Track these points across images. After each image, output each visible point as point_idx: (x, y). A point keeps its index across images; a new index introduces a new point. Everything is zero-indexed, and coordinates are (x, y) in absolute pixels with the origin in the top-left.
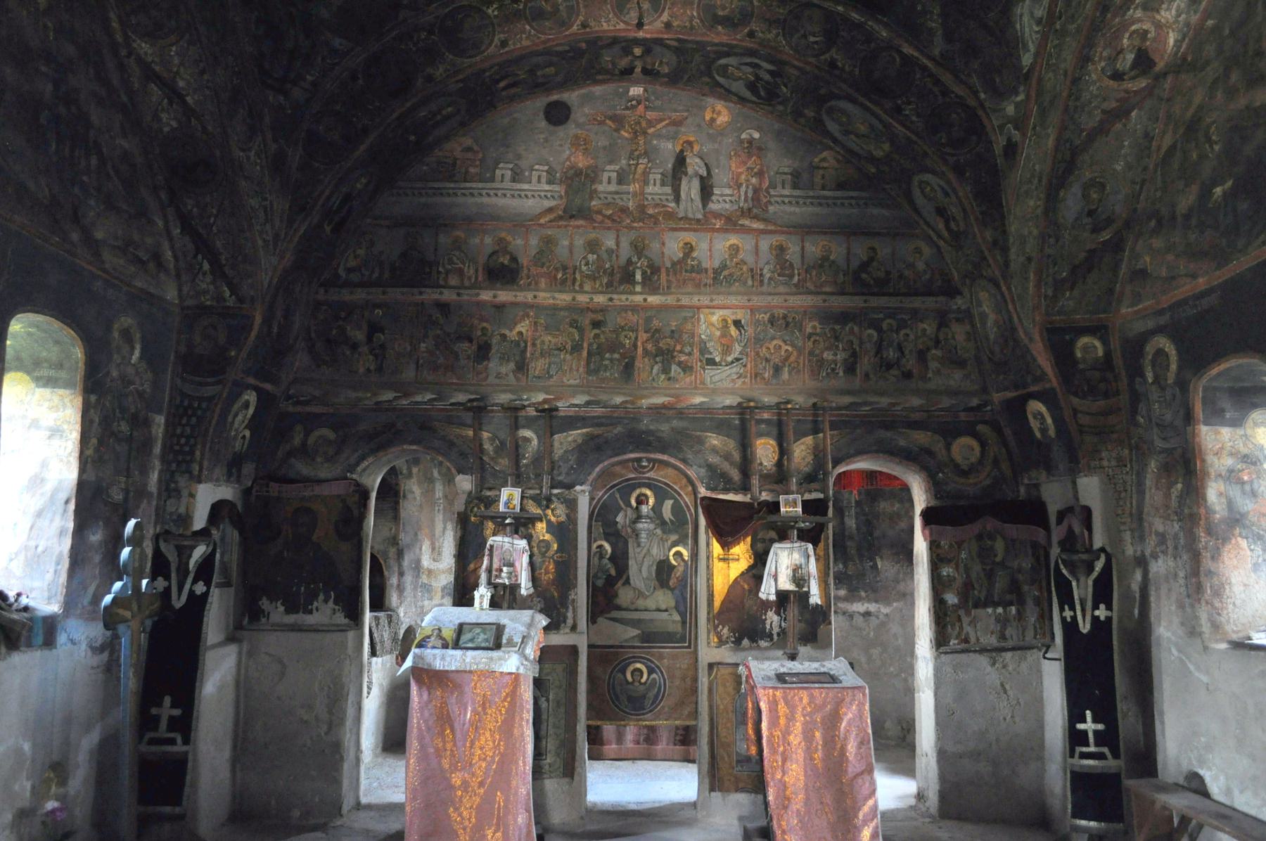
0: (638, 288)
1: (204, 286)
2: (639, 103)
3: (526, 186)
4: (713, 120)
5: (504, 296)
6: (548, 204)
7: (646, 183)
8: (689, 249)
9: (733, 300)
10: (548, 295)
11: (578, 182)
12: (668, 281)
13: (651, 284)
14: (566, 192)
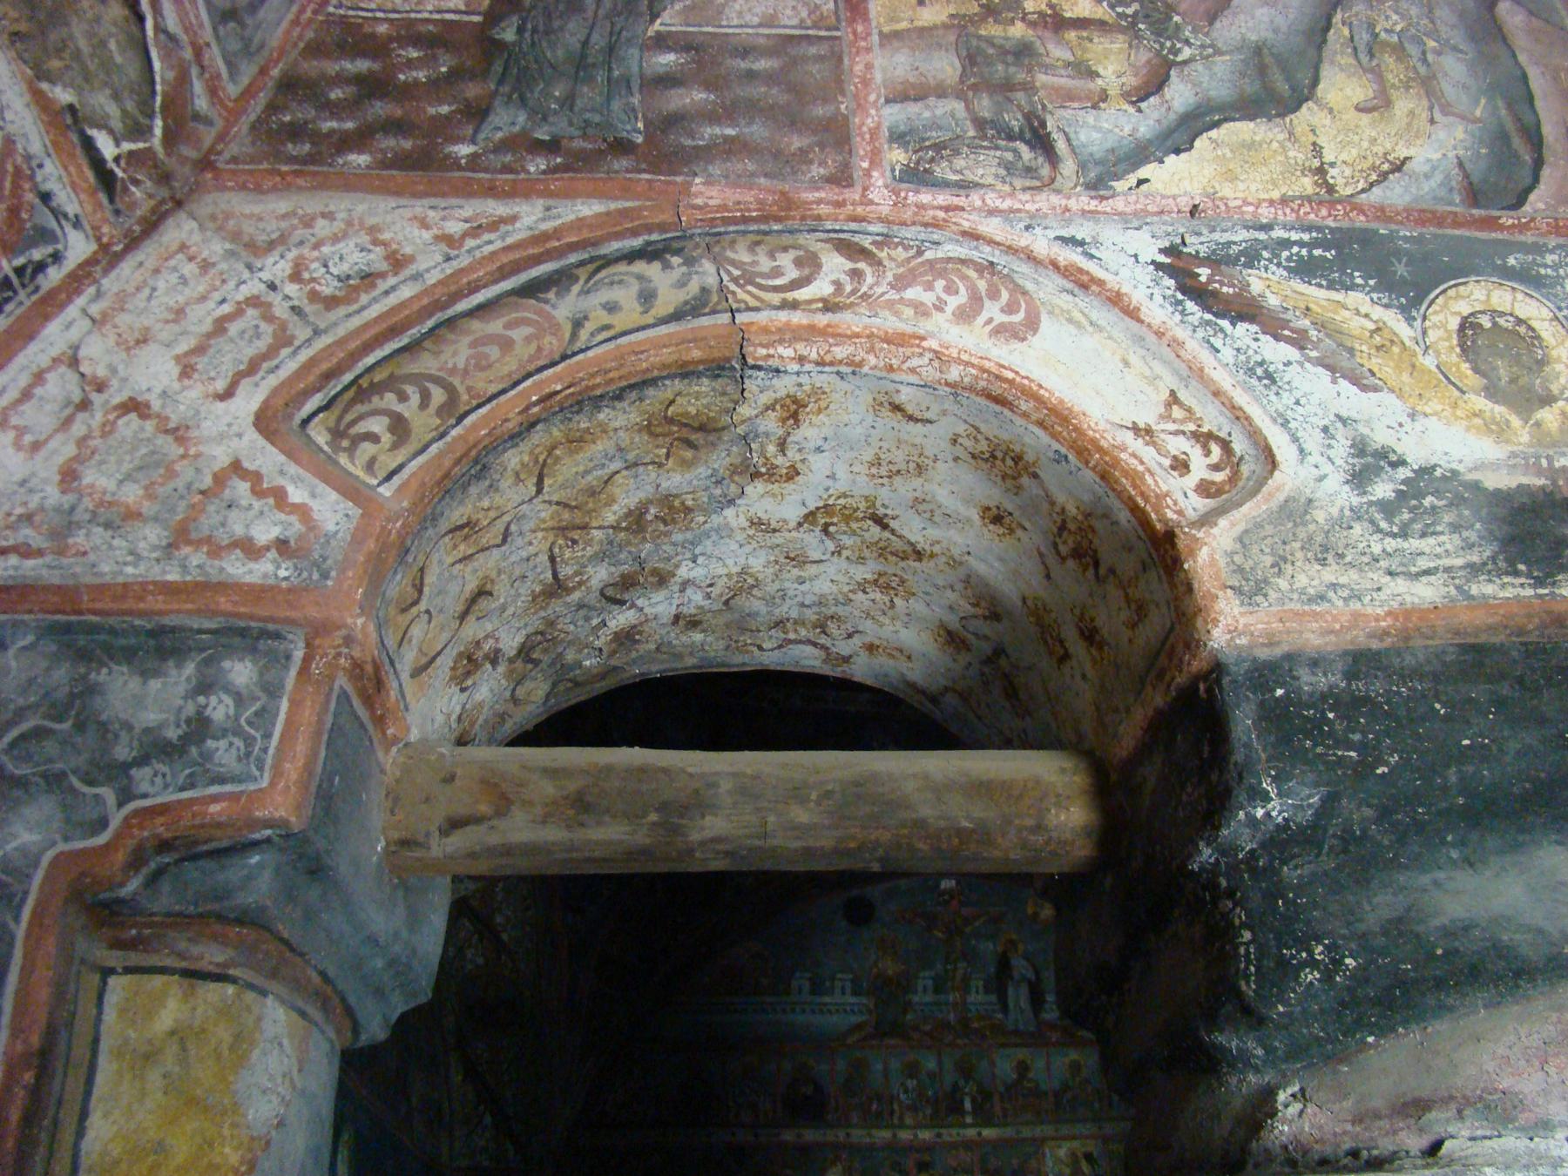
0: (969, 1120)
1: (483, 1143)
2: (952, 897)
3: (827, 999)
4: (1036, 914)
5: (810, 1135)
6: (854, 1019)
7: (965, 989)
8: (1023, 1068)
9: (1080, 1129)
10: (864, 1132)
11: (889, 992)
12: (1004, 1110)
13: (984, 1116)
14: (876, 1006)
